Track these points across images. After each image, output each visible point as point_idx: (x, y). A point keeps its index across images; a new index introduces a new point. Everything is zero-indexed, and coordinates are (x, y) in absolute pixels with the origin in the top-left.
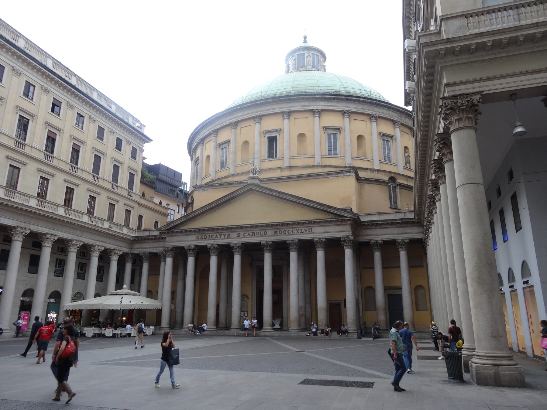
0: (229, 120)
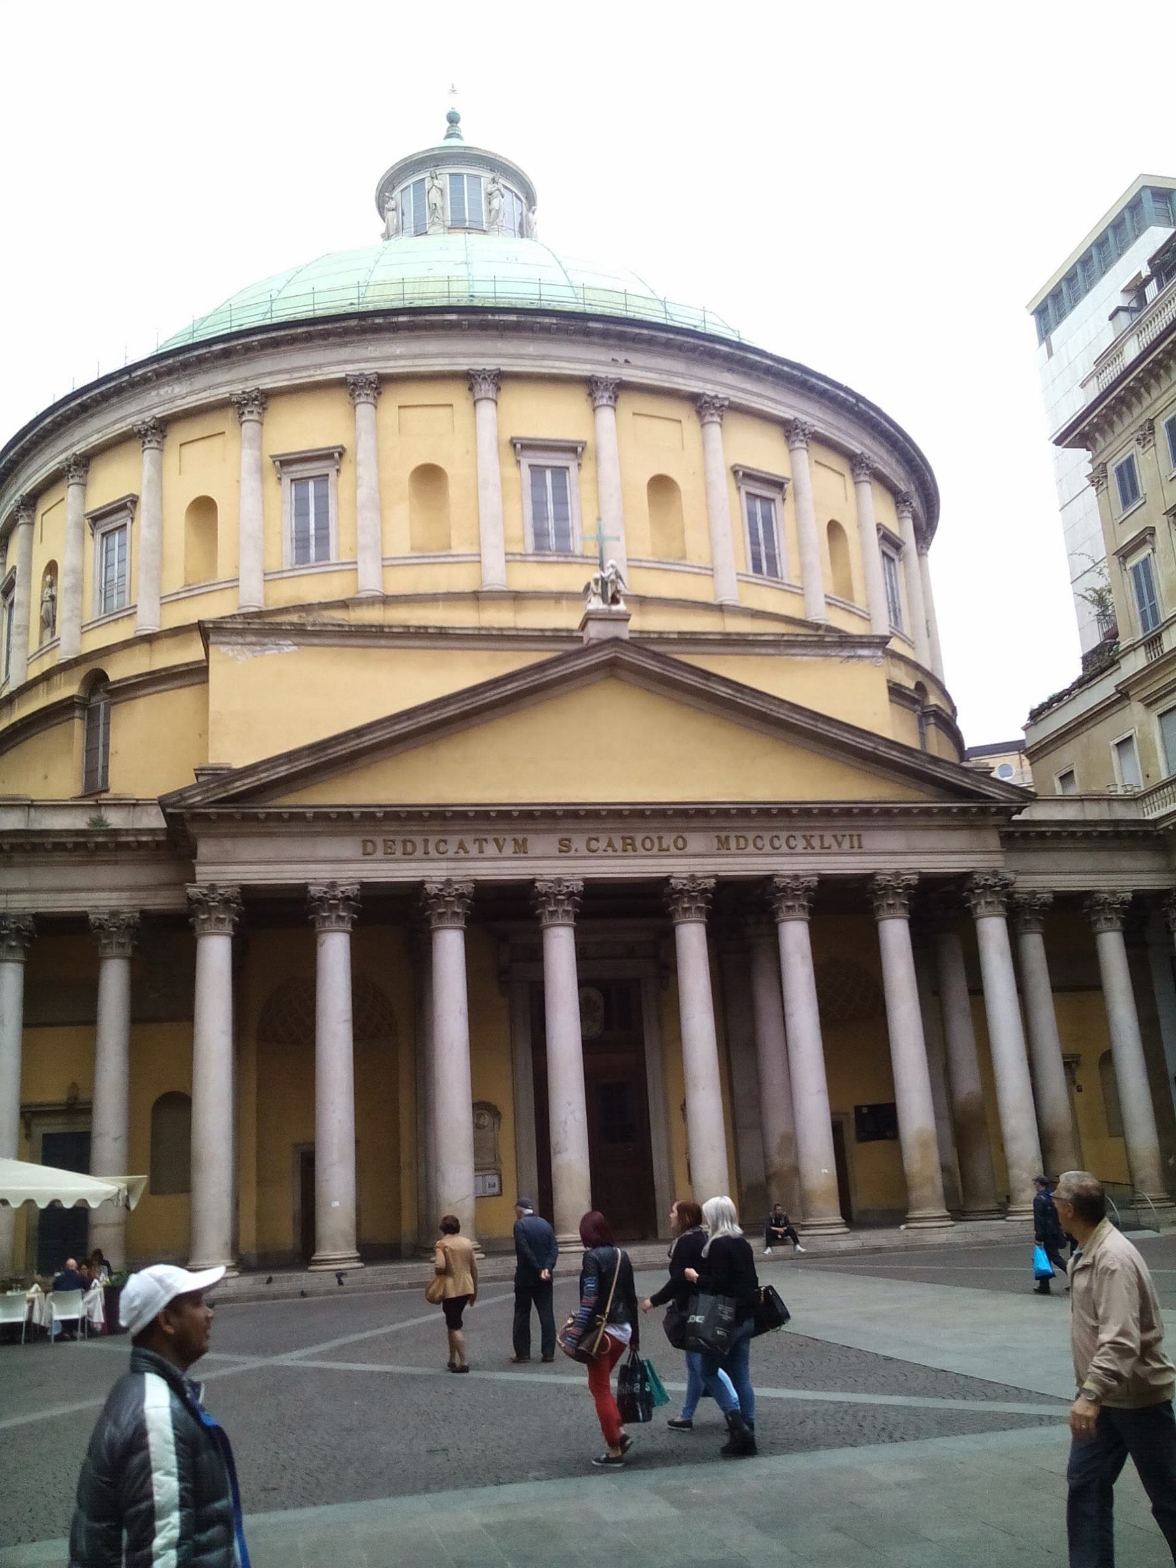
0: (339, 363)
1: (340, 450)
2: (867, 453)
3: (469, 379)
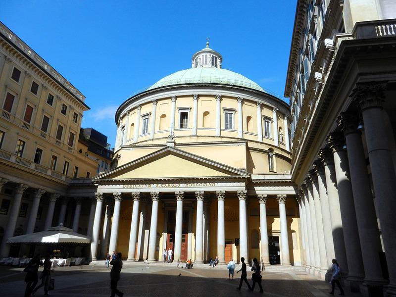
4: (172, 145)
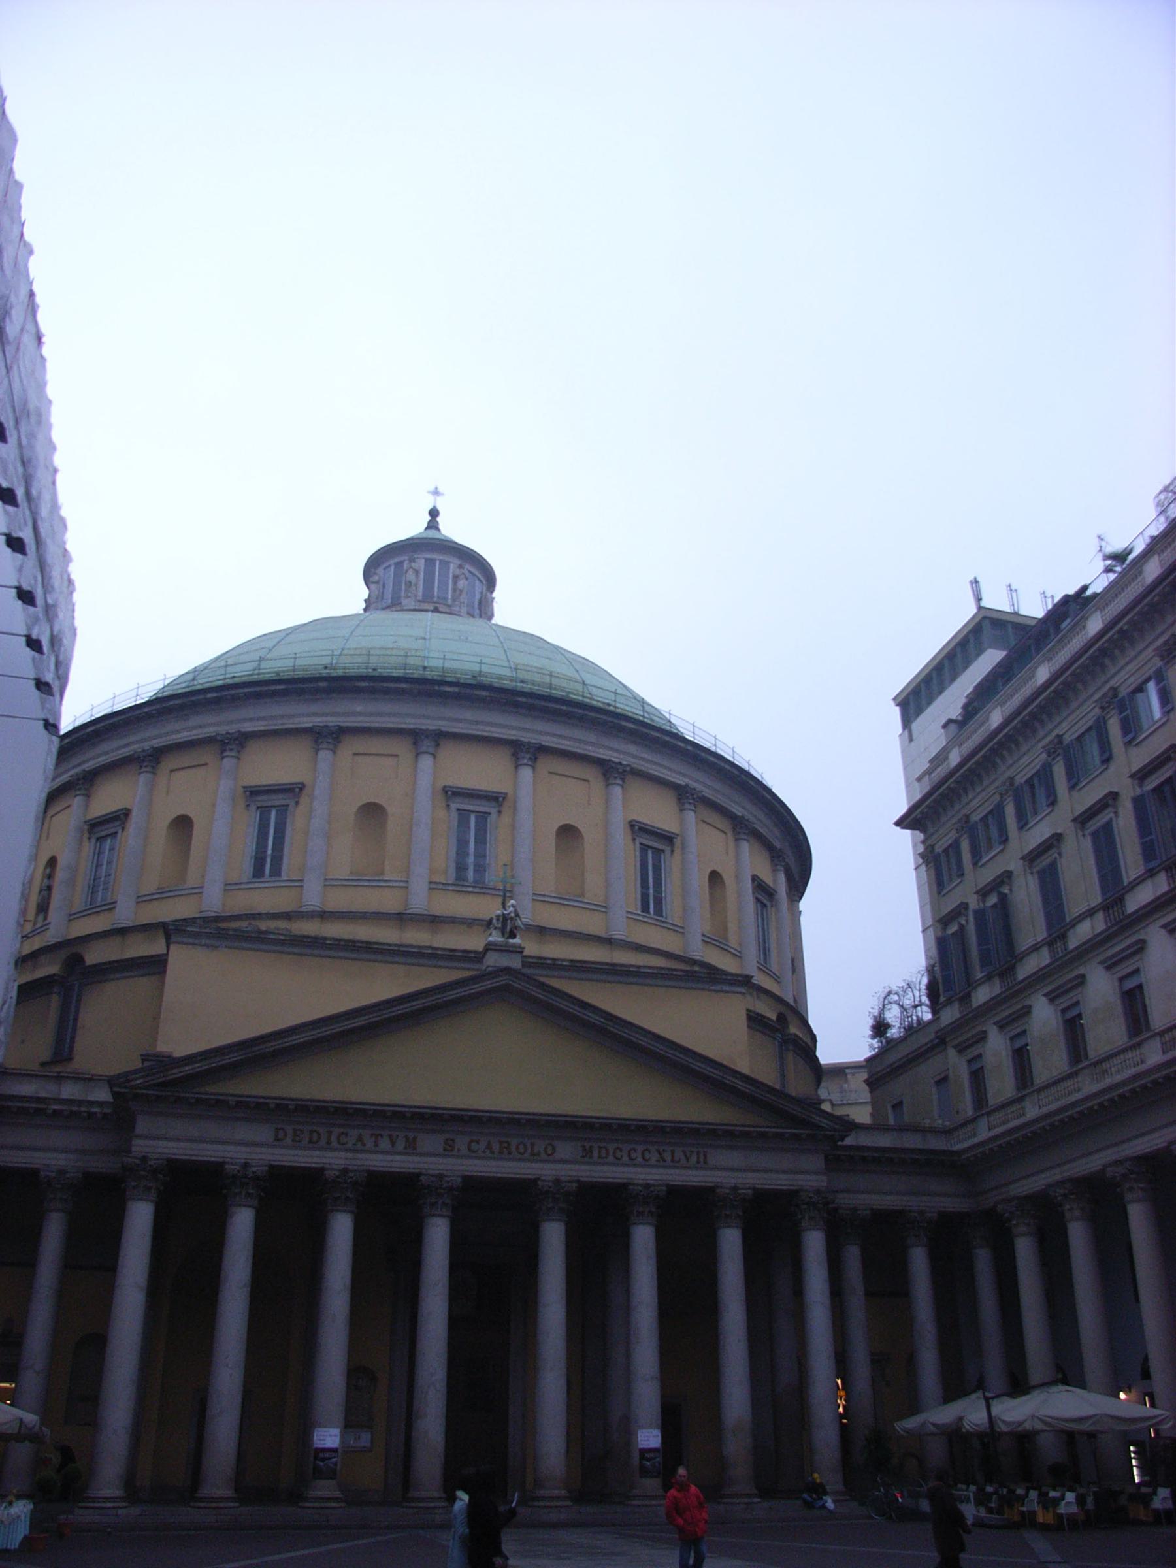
0: (309, 715)
1: (300, 786)
2: (748, 816)
3: (416, 737)
4: (515, 963)
